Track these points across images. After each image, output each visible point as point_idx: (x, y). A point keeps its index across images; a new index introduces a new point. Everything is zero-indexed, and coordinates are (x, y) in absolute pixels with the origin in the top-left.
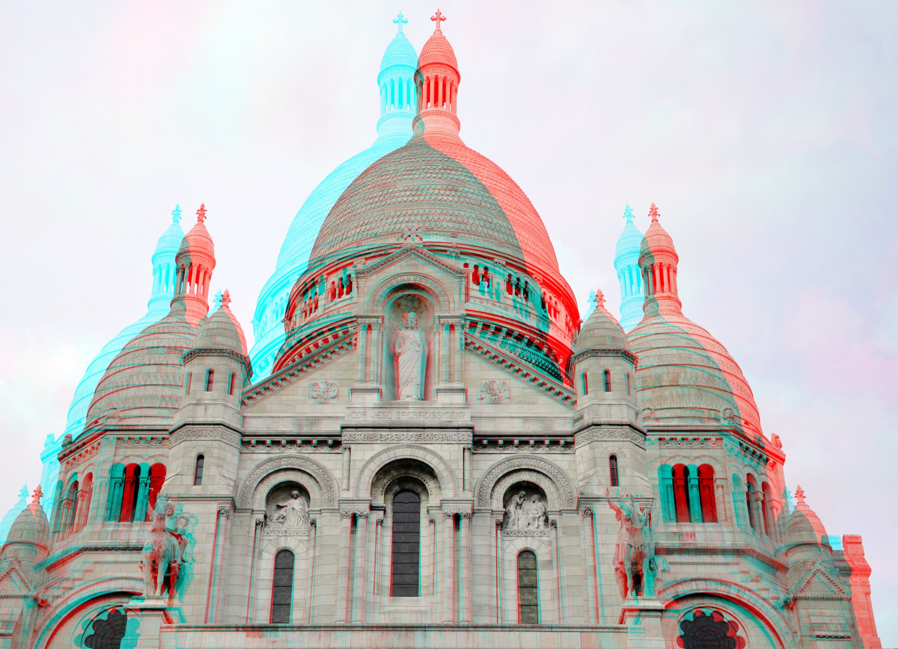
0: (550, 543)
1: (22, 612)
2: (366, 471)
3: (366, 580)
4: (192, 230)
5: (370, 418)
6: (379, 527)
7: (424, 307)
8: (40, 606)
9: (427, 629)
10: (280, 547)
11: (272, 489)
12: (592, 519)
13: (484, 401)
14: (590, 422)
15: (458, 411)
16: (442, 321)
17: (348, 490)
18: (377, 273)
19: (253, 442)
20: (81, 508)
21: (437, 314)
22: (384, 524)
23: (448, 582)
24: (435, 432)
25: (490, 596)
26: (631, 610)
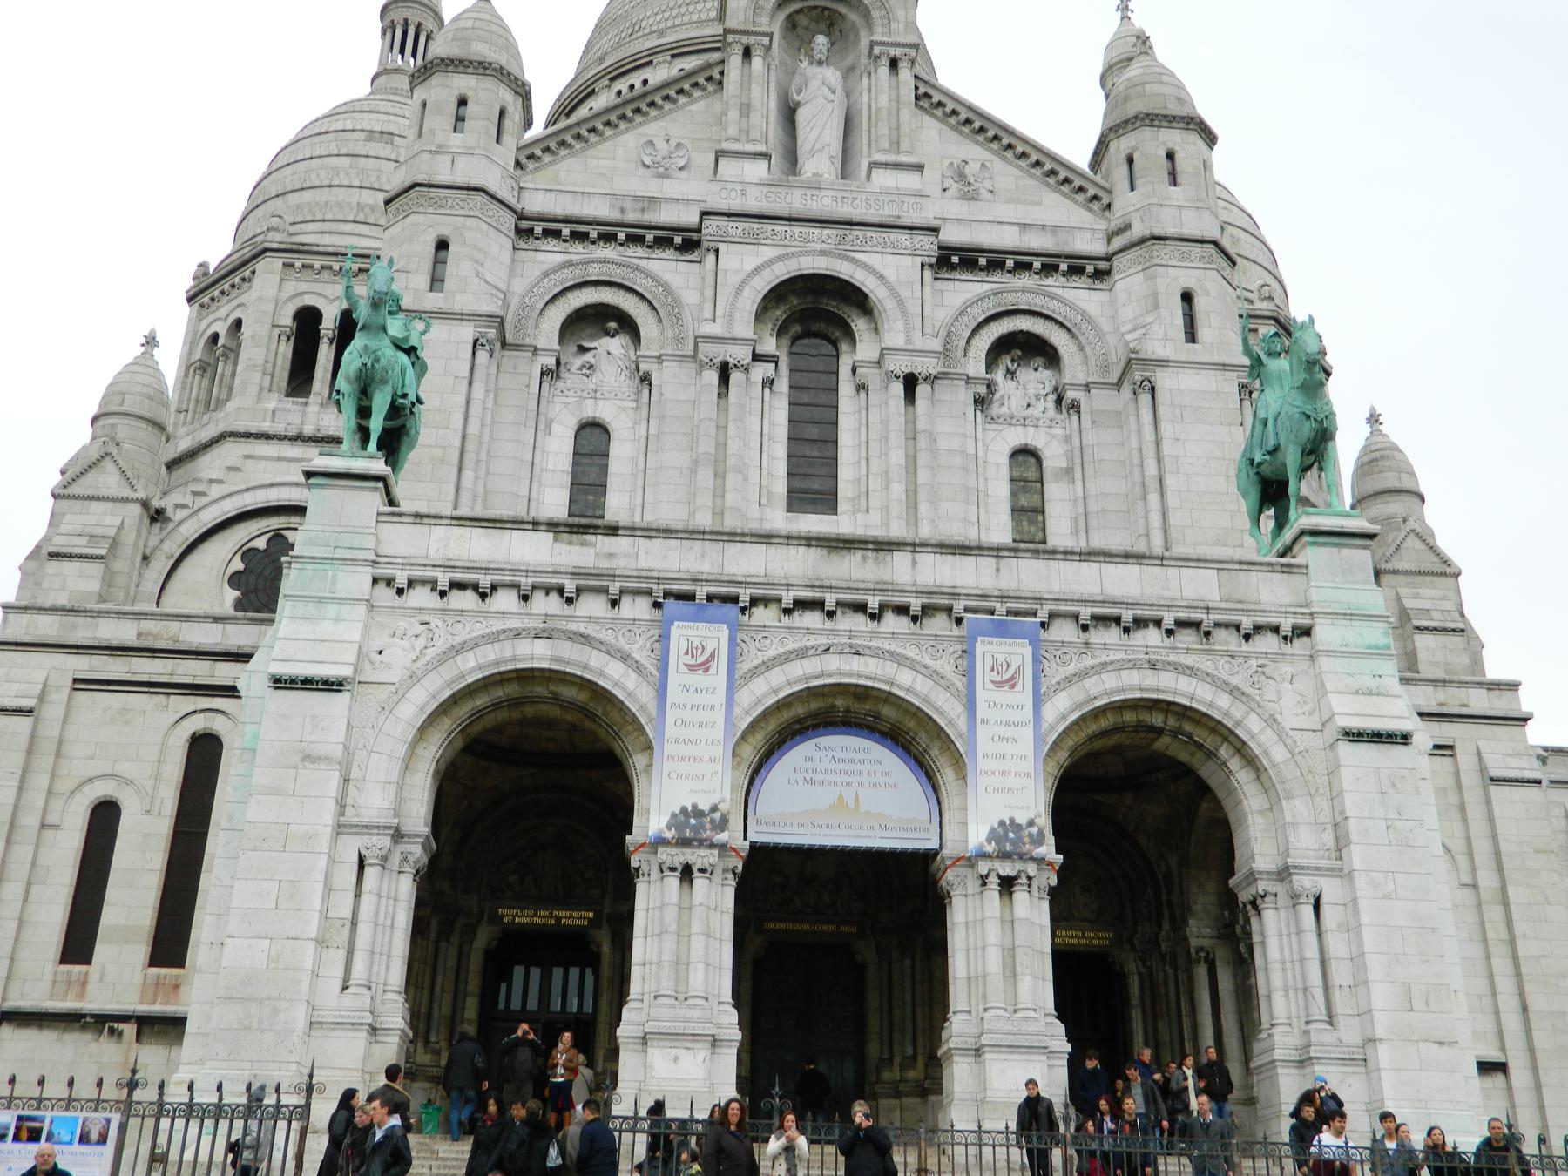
0: (1068, 439)
1: (122, 522)
2: (747, 289)
3: (746, 479)
5: (754, 201)
6: (767, 390)
7: (838, 33)
8: (153, 520)
9: (918, 549)
11: (570, 316)
14: (1147, 233)
15: (912, 200)
16: (877, 50)
19: (538, 230)
20: (223, 375)
21: (864, 43)
22: (774, 387)
23: (898, 490)
24: (871, 233)
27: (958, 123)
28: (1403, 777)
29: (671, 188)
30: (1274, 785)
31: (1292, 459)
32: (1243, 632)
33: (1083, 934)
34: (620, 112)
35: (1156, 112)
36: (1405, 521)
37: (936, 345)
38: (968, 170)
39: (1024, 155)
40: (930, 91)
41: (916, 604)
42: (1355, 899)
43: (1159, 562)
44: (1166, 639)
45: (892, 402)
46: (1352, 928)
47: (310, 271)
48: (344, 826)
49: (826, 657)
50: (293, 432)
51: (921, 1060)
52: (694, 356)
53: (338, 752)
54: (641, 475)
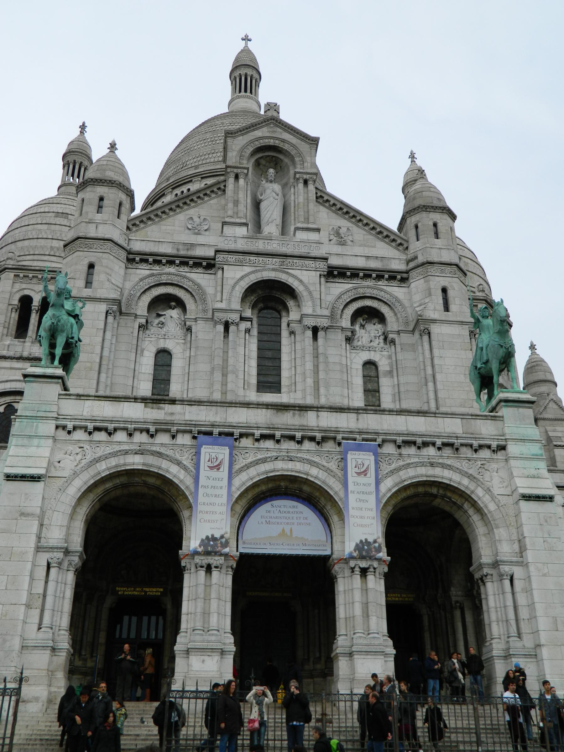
0: (390, 357)
2: (237, 287)
3: (237, 377)
4: (76, 138)
5: (241, 245)
6: (247, 334)
7: (279, 168)
9: (320, 410)
10: (160, 347)
12: (430, 337)
13: (332, 242)
15: (315, 245)
16: (298, 176)
17: (222, 302)
18: (242, 135)
19: (137, 259)
21: (292, 172)
23: (310, 381)
25: (342, 396)
26: (507, 401)
27: (336, 209)
28: (550, 517)
29: (200, 239)
30: (490, 522)
31: (494, 366)
32: (474, 448)
33: (401, 595)
34: (176, 204)
35: (428, 205)
36: (548, 395)
37: (327, 313)
38: (341, 231)
39: (367, 224)
40: (323, 195)
41: (319, 436)
42: (529, 577)
43: (433, 415)
44: (438, 452)
45: (306, 339)
46: (528, 591)
47: (27, 279)
48: (40, 548)
49: (276, 462)
50: (18, 355)
51: (323, 659)
52: (212, 318)
53: (38, 511)
54: (187, 375)
